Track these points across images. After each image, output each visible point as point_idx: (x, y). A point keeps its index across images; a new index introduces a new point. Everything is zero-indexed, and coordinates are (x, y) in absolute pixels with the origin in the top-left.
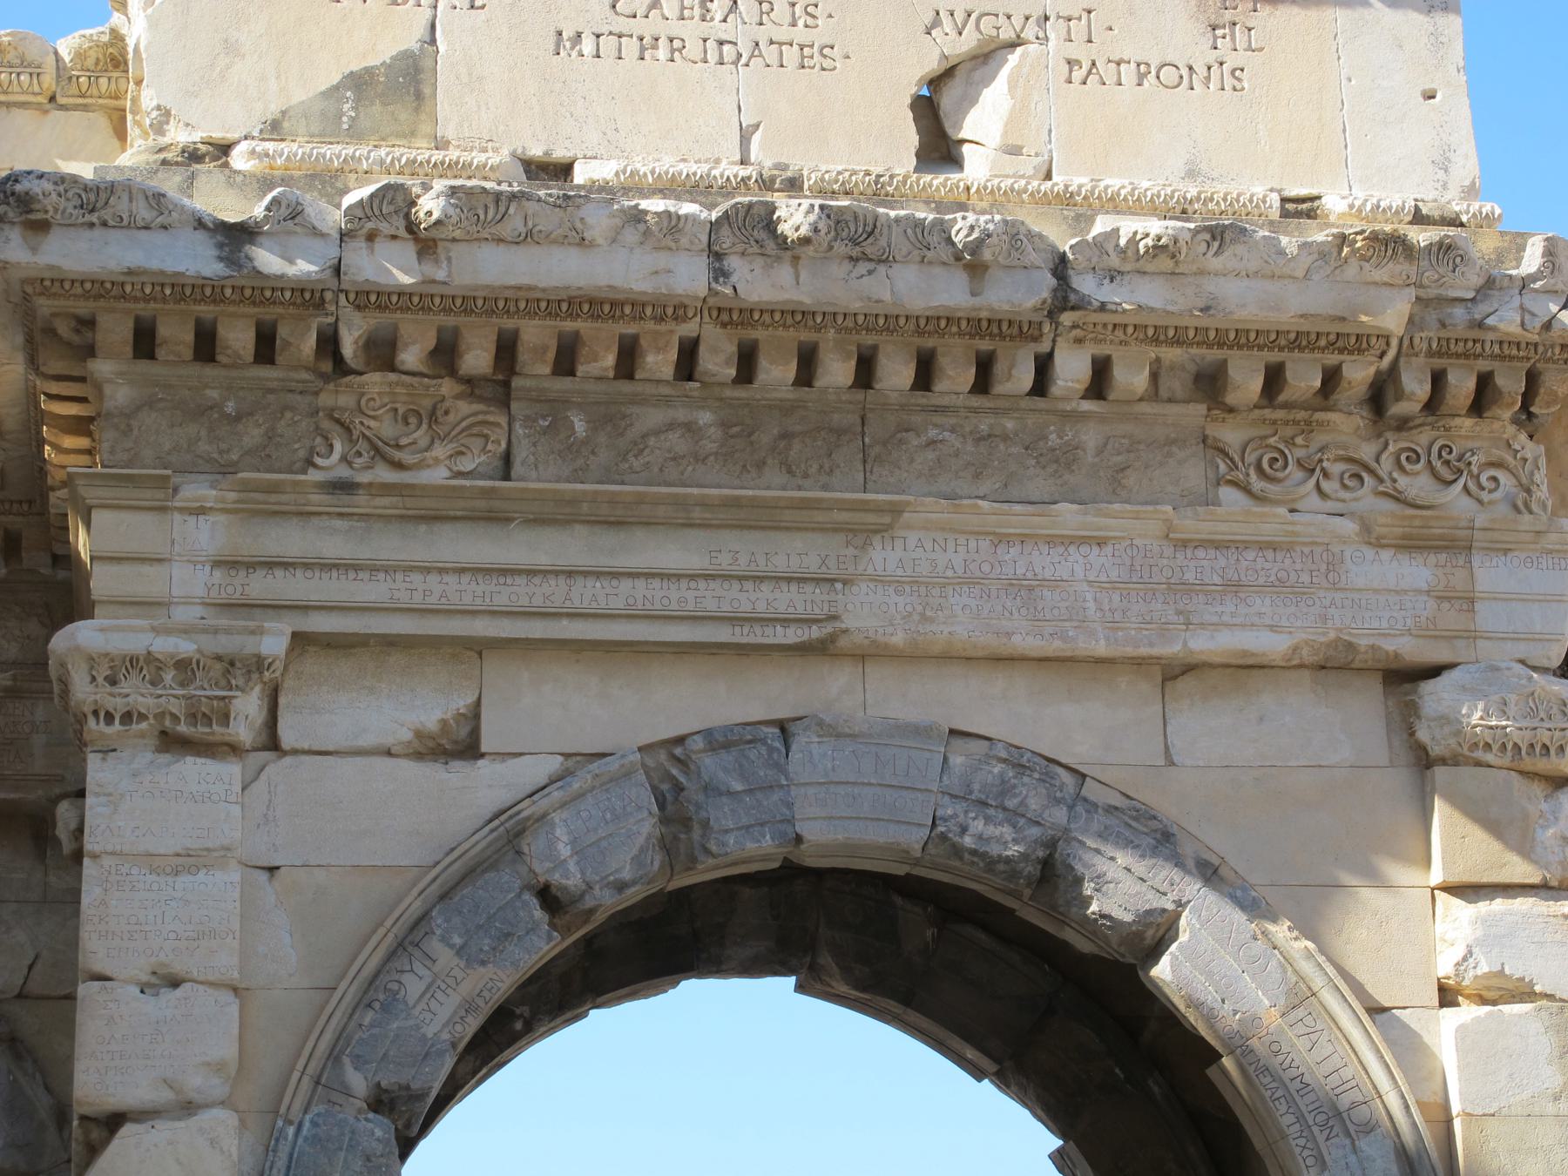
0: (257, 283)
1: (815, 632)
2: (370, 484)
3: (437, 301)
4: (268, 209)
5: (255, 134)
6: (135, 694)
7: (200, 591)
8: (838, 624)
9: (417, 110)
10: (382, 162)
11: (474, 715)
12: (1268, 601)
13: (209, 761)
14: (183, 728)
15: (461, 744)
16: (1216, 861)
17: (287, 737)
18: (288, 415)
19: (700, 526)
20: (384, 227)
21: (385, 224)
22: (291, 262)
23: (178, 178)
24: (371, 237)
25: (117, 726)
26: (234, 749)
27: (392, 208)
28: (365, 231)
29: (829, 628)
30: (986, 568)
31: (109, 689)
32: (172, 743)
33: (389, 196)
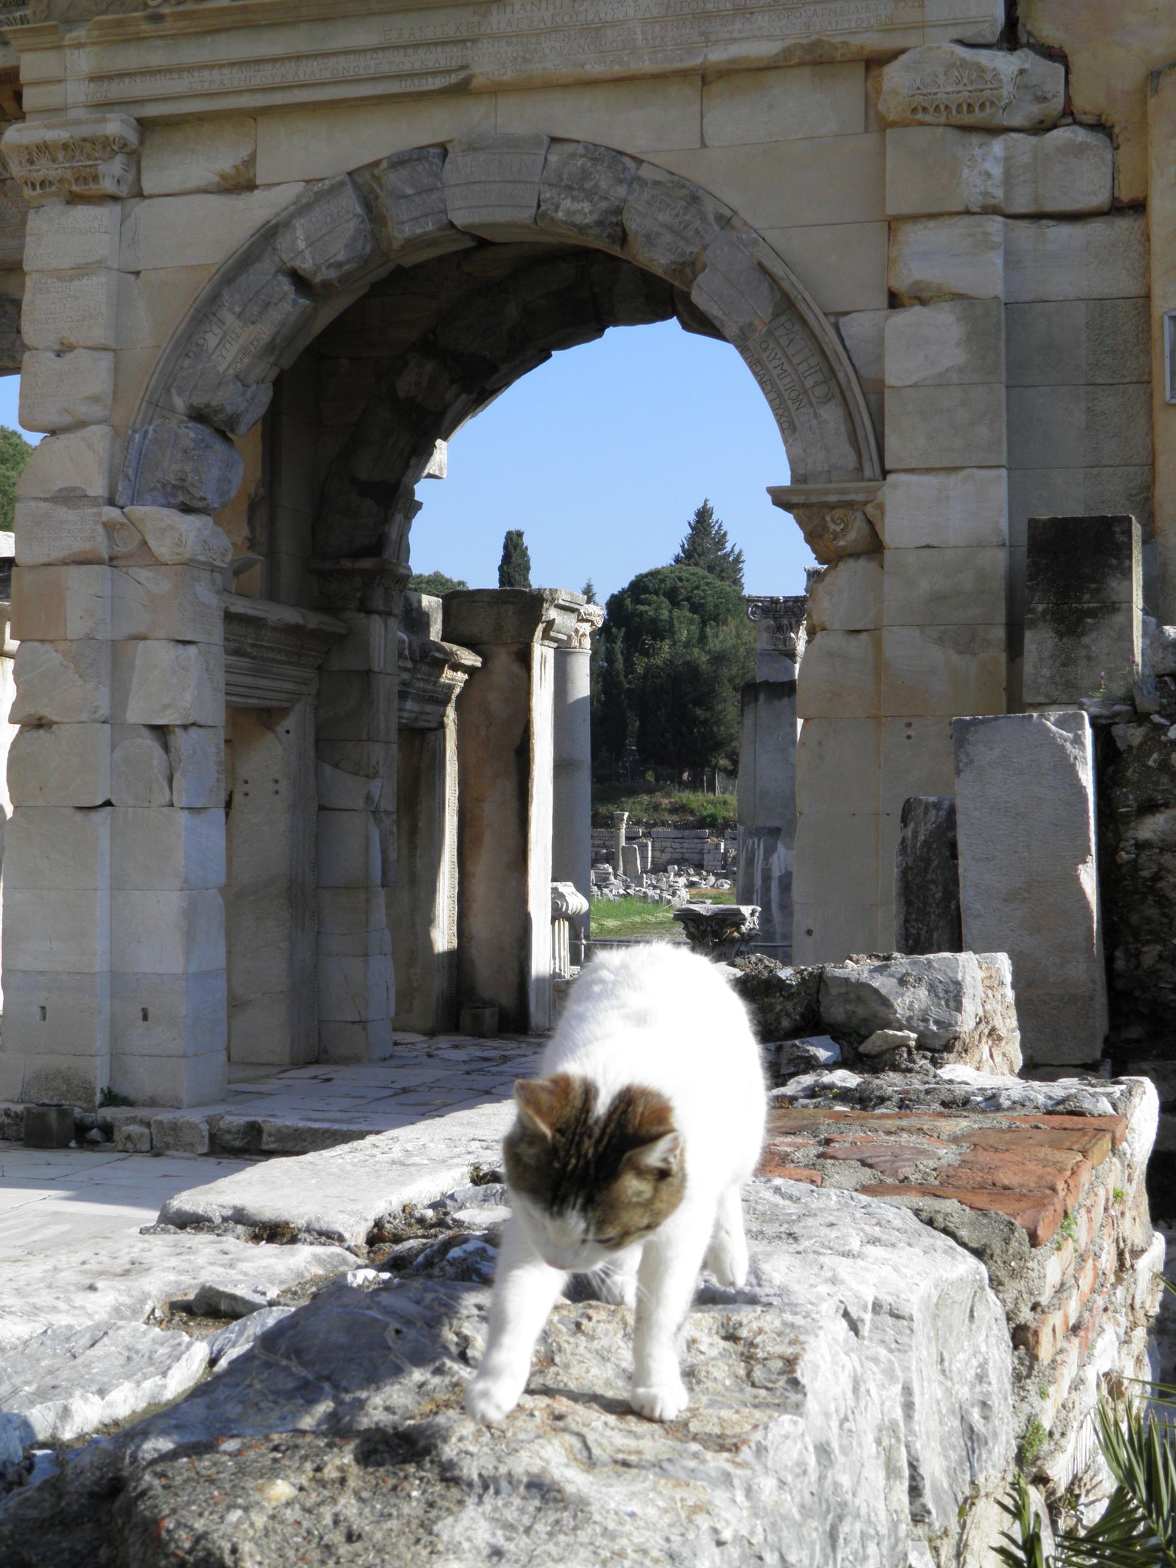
1: (454, 79)
6: (45, 169)
7: (82, 98)
8: (468, 72)
11: (250, 162)
12: (766, 18)
13: (90, 207)
15: (240, 183)
16: (728, 213)
17: (147, 188)
19: (379, 14)
25: (38, 190)
29: (462, 75)
30: (567, 18)
31: (29, 167)
32: (74, 199)
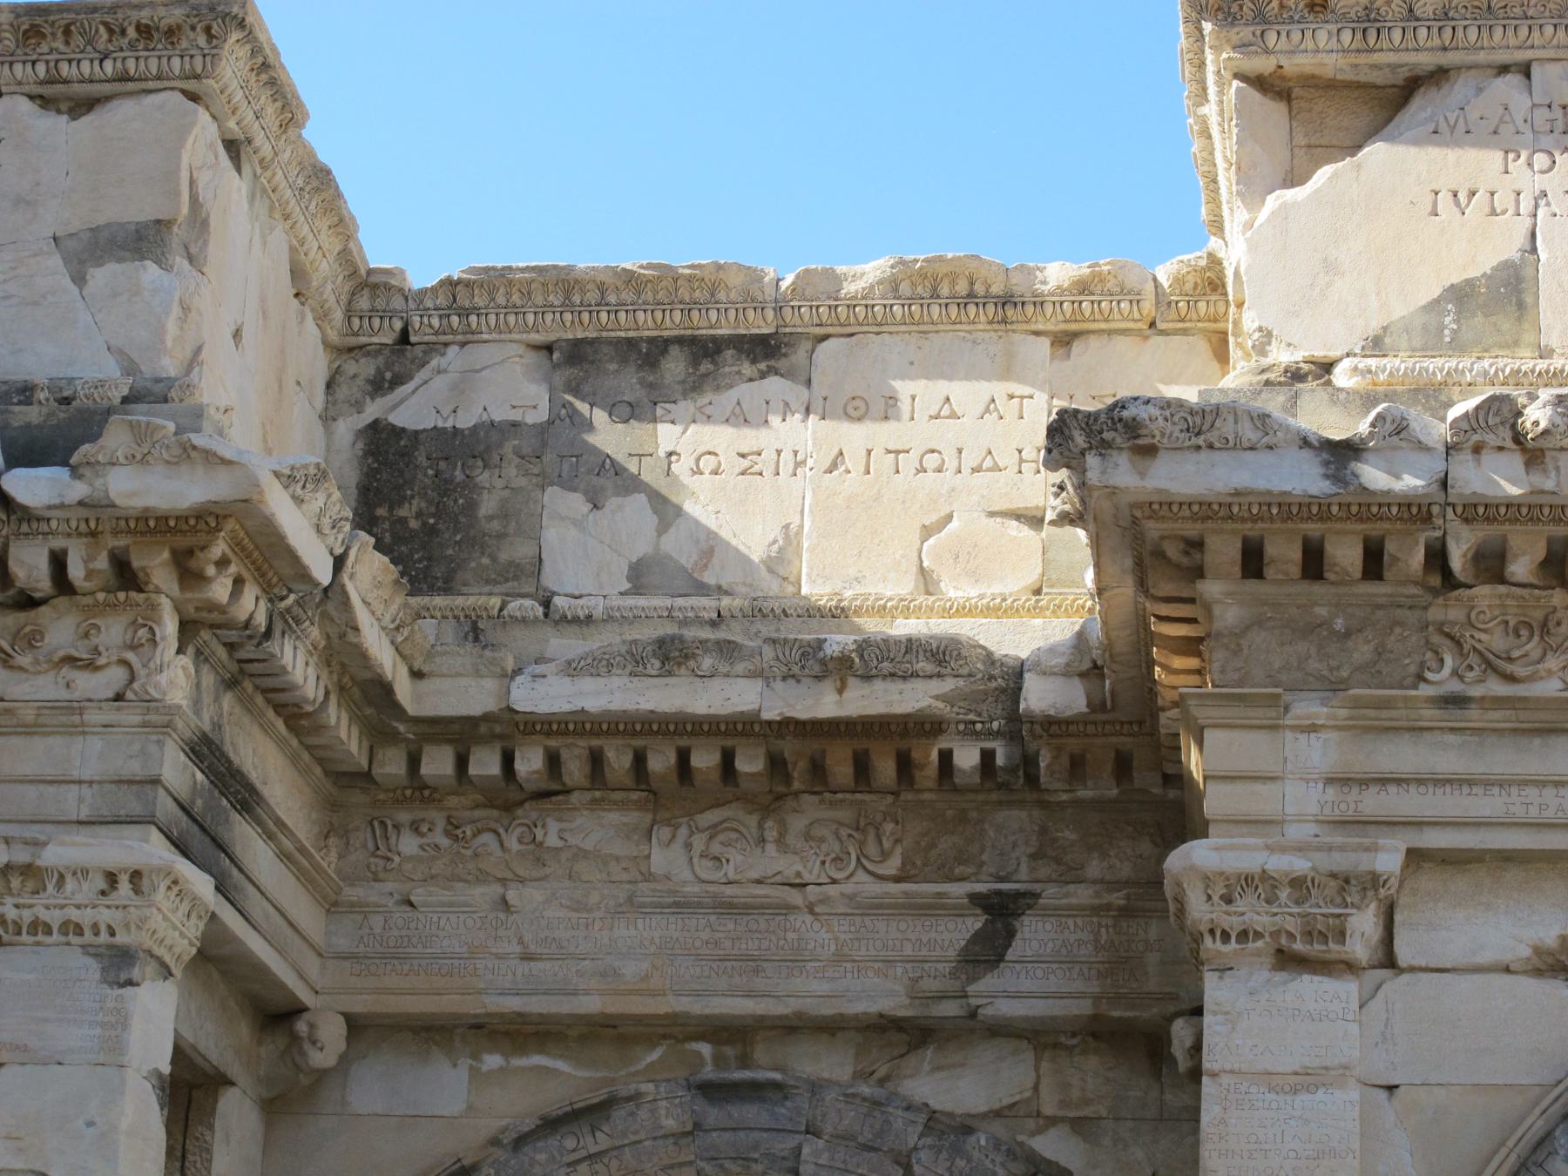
0: (1365, 499)
2: (1483, 698)
3: (1546, 511)
4: (1373, 425)
5: (1357, 351)
6: (1251, 912)
7: (1313, 809)
9: (1520, 319)
10: (1486, 373)
13: (1326, 979)
14: (1298, 946)
17: (1405, 952)
18: (1398, 630)
20: (1490, 439)
21: (1492, 436)
22: (1398, 477)
23: (1281, 399)
24: (1477, 449)
25: (1233, 945)
26: (1349, 967)
27: (1498, 420)
28: (1471, 443)
31: (1225, 907)
32: (1288, 961)
33: (1494, 408)
